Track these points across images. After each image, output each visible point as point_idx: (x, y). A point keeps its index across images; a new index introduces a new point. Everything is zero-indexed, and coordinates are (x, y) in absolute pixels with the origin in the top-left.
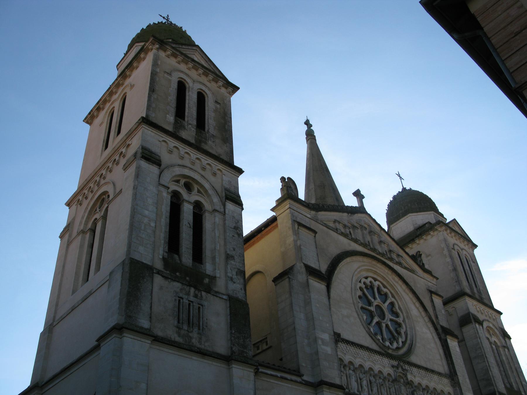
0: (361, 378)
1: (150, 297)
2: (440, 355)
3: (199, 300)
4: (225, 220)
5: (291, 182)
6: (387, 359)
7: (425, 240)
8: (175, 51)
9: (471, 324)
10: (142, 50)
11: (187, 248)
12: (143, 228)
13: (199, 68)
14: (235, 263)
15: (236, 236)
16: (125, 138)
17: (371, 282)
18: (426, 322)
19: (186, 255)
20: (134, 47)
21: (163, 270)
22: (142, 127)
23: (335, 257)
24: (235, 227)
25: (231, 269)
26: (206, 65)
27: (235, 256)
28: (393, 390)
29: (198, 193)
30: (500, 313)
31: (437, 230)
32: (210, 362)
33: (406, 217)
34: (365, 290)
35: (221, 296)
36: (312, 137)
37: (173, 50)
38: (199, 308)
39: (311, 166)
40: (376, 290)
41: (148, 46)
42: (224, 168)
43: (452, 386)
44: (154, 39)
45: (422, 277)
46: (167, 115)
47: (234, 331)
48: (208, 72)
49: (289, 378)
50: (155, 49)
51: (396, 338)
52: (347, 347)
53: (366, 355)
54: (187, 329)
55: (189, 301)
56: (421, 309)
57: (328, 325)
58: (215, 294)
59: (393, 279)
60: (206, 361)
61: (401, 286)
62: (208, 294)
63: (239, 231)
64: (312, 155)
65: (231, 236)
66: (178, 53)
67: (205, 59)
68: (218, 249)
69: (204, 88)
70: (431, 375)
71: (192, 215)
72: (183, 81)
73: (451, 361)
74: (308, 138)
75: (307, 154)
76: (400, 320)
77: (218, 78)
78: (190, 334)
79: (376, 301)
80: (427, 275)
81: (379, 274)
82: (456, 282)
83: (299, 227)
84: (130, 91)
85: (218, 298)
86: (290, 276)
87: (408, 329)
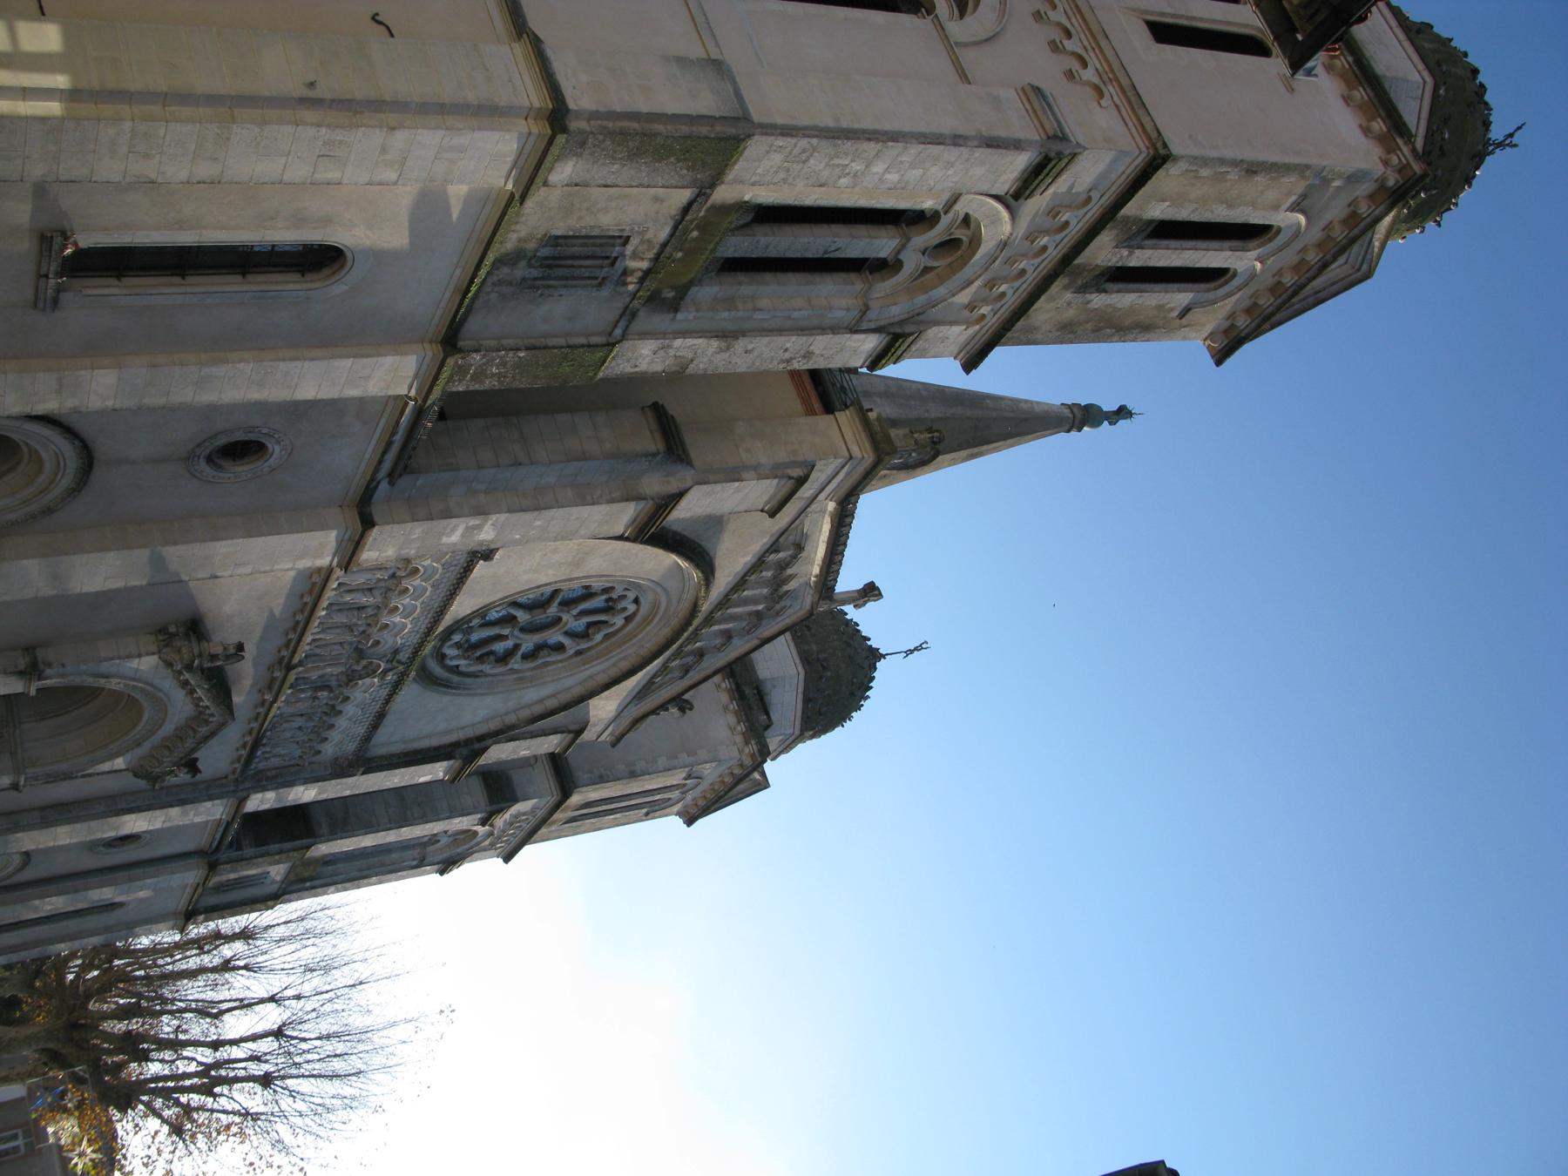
0: (373, 591)
1: (635, 184)
2: (414, 740)
3: (616, 278)
4: (835, 329)
5: (927, 458)
6: (415, 641)
7: (726, 708)
8: (1363, 224)
9: (488, 803)
10: (1397, 125)
11: (767, 247)
12: (836, 161)
13: (1300, 278)
14: (710, 354)
15: (787, 356)
16: (1125, 82)
17: (625, 609)
18: (504, 717)
19: (746, 244)
20: (1426, 74)
21: (710, 203)
22: (1141, 153)
23: (700, 546)
24: (813, 353)
25: (695, 345)
26: (1308, 289)
27: (728, 355)
28: (338, 650)
29: (922, 268)
30: (508, 858)
31: (747, 743)
32: (443, 304)
33: (798, 661)
34: (604, 597)
35: (622, 323)
36: (1077, 422)
37: (1368, 220)
38: (597, 278)
39: (994, 414)
40: (602, 617)
41: (1399, 153)
42: (985, 329)
43: (336, 759)
44: (1415, 178)
45: (622, 714)
46: (1167, 204)
47: (522, 354)
49: (386, 457)
50: (1385, 173)
51: (470, 653)
52: (456, 565)
53: (433, 602)
54: (539, 257)
55: (616, 258)
56: (538, 709)
57: (517, 537)
58: (628, 312)
59: (626, 656)
60: (448, 295)
61: (603, 671)
62: (632, 297)
63: (799, 362)
64: (1026, 420)
65: (788, 345)
66: (1356, 231)
67: (1324, 289)
68: (755, 317)
69: (1235, 283)
70: (367, 723)
71: (861, 256)
72: (1270, 235)
73: (397, 763)
74: (1076, 410)
75: (1031, 402)
76: (515, 663)
78: (523, 263)
79: (571, 620)
80: (625, 725)
83: (792, 481)
84: (1278, 74)
85: (618, 317)
86: (660, 456)
87: (490, 679)
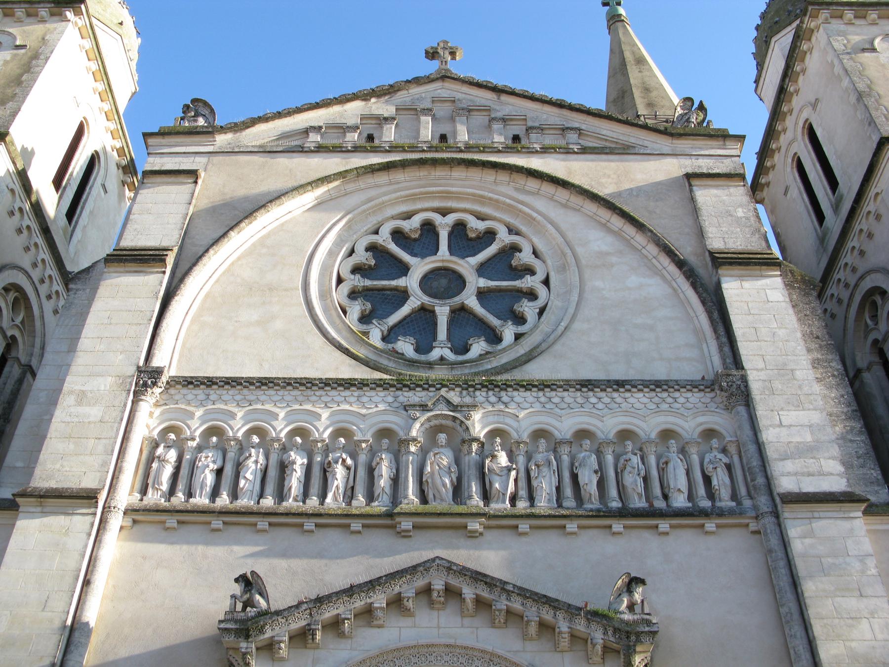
48: (11, 6)
77: (33, 6)
80: (695, 142)
81: (460, 193)
82: (870, 124)
